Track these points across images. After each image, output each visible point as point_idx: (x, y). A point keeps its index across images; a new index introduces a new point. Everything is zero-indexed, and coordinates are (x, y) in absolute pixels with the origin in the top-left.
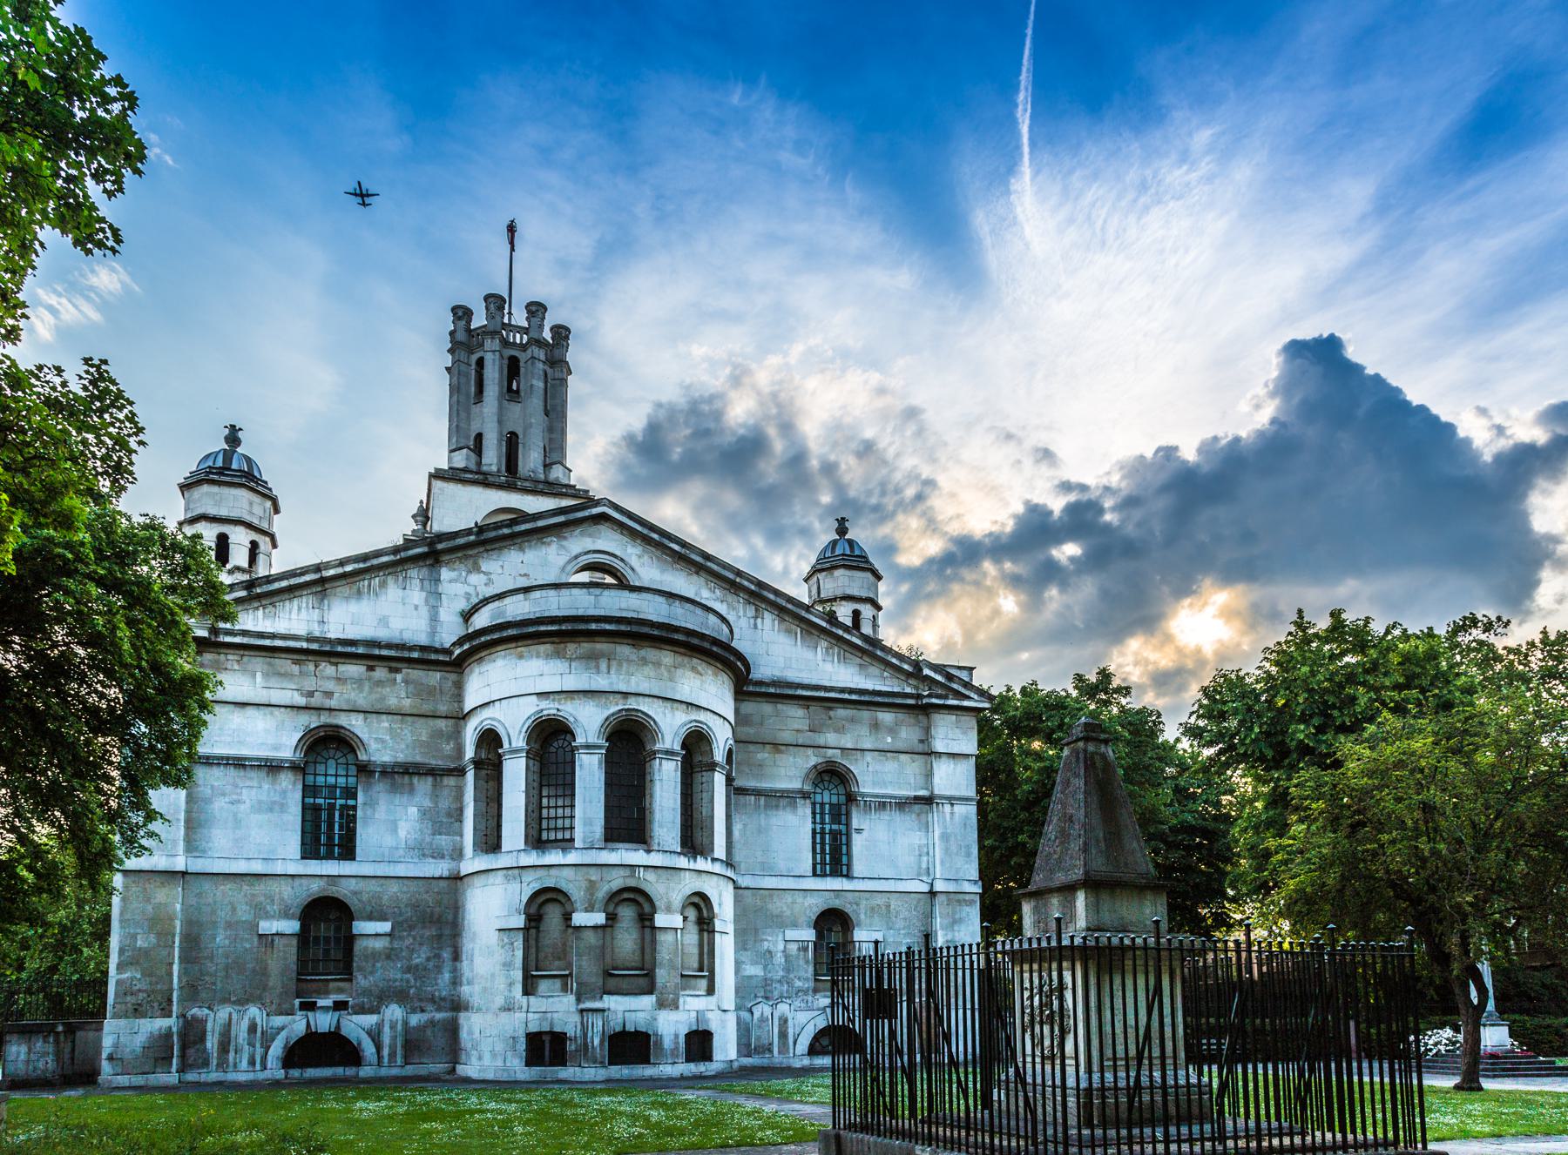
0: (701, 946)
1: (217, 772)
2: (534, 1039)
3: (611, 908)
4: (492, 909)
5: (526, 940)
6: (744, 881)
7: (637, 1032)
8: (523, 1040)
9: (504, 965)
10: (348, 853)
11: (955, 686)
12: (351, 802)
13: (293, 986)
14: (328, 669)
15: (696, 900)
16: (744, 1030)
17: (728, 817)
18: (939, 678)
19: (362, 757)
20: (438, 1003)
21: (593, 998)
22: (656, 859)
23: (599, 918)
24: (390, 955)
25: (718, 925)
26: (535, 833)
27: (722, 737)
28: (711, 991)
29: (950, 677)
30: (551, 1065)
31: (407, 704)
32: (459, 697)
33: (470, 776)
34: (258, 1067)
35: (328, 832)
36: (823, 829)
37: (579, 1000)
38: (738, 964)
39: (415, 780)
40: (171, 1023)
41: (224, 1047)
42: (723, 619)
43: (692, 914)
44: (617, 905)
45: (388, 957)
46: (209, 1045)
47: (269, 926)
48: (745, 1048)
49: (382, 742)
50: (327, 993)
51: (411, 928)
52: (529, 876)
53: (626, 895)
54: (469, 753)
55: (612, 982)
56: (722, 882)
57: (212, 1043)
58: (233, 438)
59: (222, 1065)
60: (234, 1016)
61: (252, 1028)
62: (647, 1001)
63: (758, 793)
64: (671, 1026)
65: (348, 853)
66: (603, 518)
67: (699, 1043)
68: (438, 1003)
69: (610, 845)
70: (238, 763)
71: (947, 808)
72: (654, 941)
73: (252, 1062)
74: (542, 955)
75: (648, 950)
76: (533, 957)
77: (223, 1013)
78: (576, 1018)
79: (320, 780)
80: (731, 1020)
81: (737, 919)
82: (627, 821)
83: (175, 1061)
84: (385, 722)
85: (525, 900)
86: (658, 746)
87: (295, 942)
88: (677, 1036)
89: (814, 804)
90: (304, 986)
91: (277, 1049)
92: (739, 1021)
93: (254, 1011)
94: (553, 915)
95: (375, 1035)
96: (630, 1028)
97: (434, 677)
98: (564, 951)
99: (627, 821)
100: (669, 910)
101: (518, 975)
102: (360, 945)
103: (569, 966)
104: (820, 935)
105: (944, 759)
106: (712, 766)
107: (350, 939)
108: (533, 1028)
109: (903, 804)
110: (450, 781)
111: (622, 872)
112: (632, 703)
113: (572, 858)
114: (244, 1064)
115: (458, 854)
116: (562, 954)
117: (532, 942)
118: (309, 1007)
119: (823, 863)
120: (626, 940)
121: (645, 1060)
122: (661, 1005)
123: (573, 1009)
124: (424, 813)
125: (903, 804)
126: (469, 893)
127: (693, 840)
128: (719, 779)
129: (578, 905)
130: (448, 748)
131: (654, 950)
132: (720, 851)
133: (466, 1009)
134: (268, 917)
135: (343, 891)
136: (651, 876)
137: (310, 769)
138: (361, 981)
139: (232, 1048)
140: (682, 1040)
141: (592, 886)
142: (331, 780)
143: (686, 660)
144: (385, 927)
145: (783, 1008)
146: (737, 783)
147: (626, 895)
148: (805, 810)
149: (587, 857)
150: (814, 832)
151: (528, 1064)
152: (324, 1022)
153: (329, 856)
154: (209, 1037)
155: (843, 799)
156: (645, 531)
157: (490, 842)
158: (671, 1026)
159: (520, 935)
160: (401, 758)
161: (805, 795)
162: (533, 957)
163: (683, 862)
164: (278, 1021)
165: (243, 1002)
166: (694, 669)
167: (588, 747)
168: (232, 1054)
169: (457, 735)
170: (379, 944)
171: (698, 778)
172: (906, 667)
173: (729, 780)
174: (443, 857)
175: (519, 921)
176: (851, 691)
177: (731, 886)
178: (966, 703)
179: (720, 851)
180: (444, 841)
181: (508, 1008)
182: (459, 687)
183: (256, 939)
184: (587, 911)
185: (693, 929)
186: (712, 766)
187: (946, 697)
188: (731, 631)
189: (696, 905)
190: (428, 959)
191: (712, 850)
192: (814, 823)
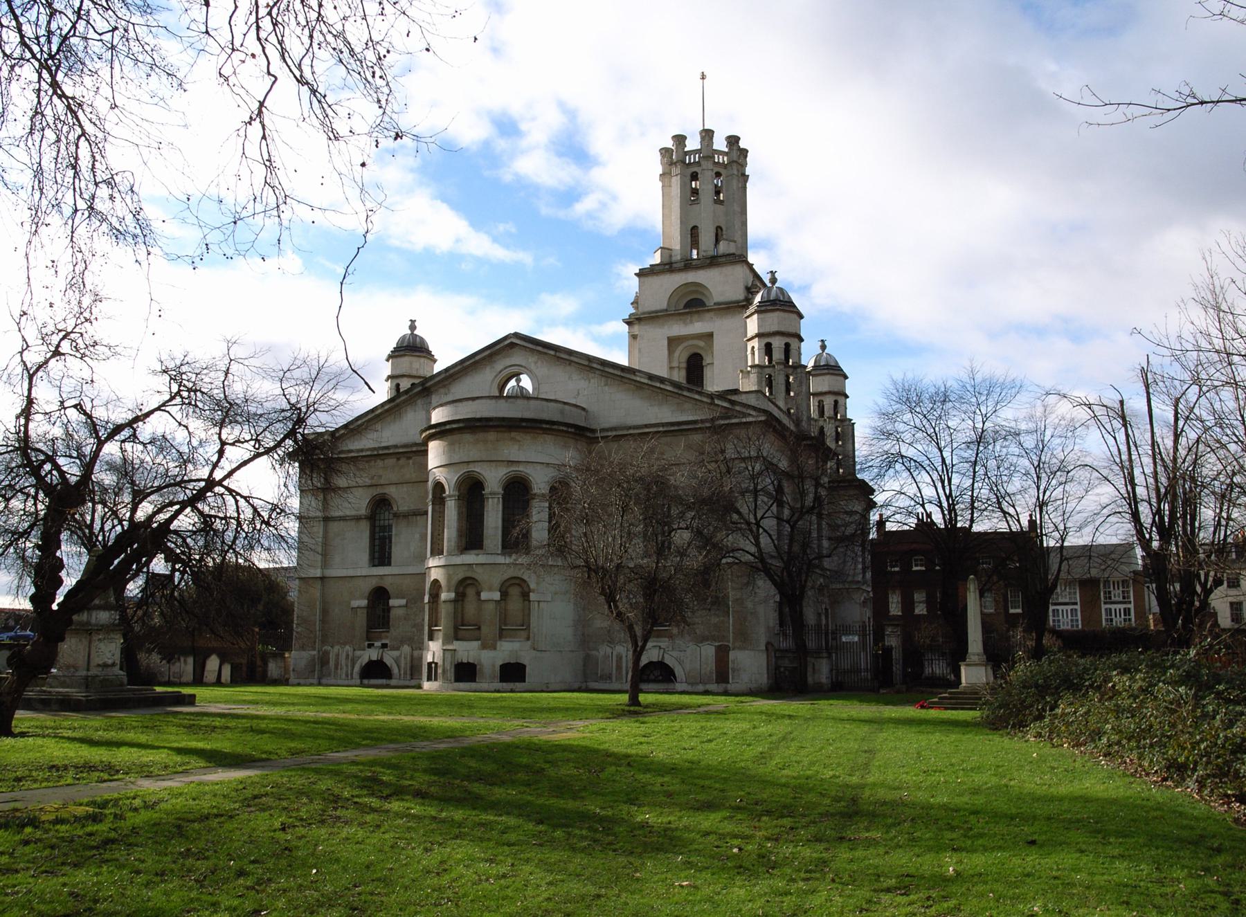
1: (336, 523)
7: (468, 663)
14: (380, 463)
41: (336, 668)
44: (465, 587)
47: (355, 603)
57: (332, 663)
58: (413, 327)
62: (476, 644)
66: (512, 345)
70: (343, 519)
84: (405, 488)
86: (487, 491)
91: (357, 669)
94: (471, 592)
95: (397, 661)
100: (490, 589)
102: (393, 613)
107: (388, 609)
112: (472, 468)
118: (370, 646)
120: (515, 605)
122: (484, 647)
135: (386, 583)
136: (479, 570)
138: (394, 632)
140: (498, 669)
144: (403, 602)
163: (501, 560)
164: (358, 653)
165: (345, 644)
166: (513, 439)
170: (401, 612)
172: (705, 400)
176: (672, 424)
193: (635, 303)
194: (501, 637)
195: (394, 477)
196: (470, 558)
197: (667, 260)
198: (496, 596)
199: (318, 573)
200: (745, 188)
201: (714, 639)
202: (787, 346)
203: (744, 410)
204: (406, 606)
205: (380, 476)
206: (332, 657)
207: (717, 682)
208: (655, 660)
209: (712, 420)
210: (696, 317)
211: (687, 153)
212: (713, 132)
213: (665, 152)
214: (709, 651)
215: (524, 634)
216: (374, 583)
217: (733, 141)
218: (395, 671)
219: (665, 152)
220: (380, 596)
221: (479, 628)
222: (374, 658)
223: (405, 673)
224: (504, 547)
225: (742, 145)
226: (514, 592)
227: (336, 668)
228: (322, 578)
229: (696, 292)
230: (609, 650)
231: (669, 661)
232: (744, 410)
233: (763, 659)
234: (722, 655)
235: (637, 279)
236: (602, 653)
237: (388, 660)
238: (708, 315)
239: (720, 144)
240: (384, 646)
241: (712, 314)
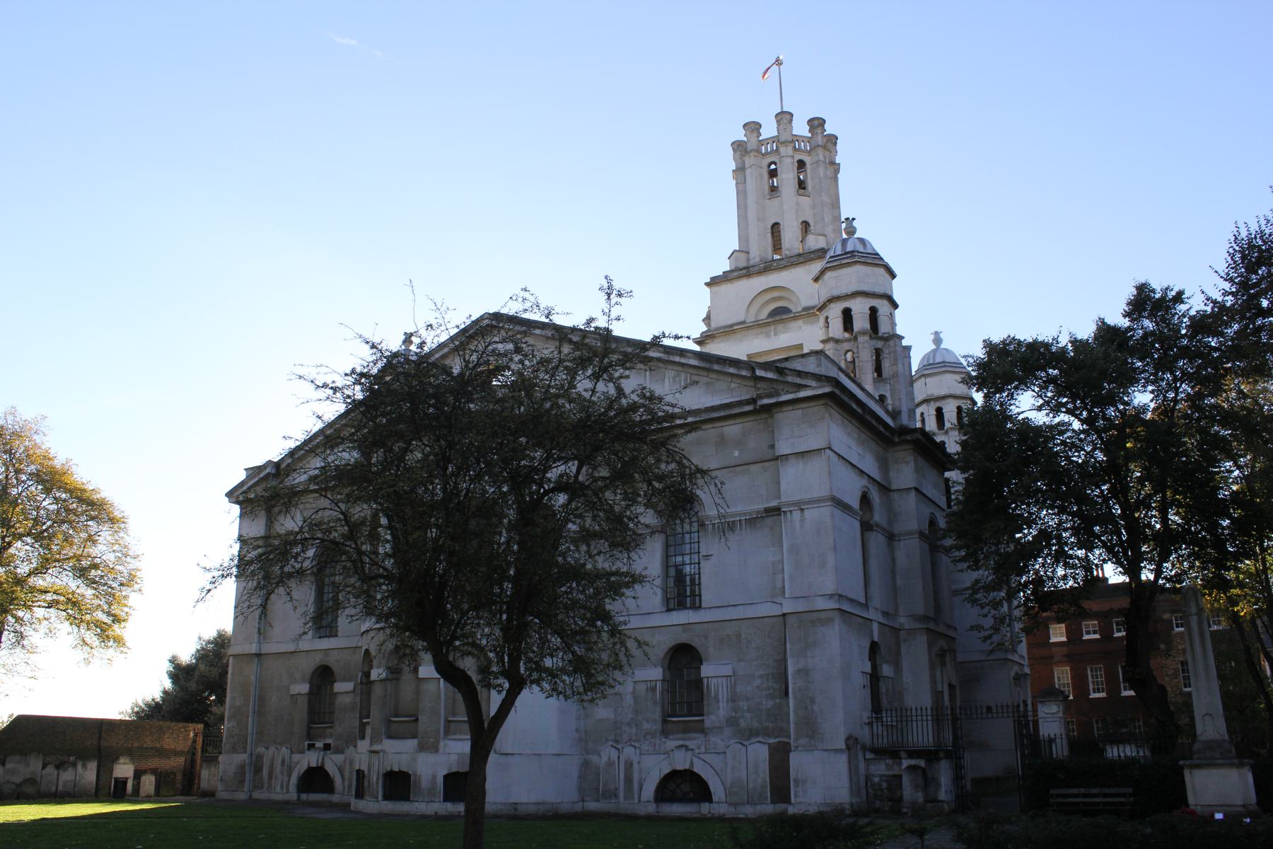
11: (790, 379)
18: (770, 375)
29: (781, 371)
37: (371, 744)
40: (242, 757)
41: (270, 778)
61: (283, 761)
62: (412, 744)
71: (797, 515)
73: (282, 787)
83: (247, 784)
88: (434, 777)
105: (792, 460)
109: (753, 521)
114: (278, 789)
118: (311, 746)
121: (406, 798)
122: (422, 748)
125: (753, 521)
135: (332, 661)
140: (440, 780)
164: (296, 757)
170: (347, 700)
172: (744, 373)
178: (803, 394)
187: (778, 395)
193: (707, 320)
194: (447, 732)
197: (743, 264)
199: (253, 649)
200: (836, 179)
201: (766, 733)
202: (873, 311)
203: (798, 381)
204: (354, 691)
206: (266, 761)
207: (773, 802)
209: (753, 401)
210: (780, 327)
211: (761, 143)
212: (792, 115)
213: (738, 147)
214: (760, 753)
216: (317, 660)
217: (817, 124)
219: (738, 147)
220: (324, 675)
221: (417, 720)
222: (314, 764)
223: (350, 787)
225: (829, 129)
227: (270, 778)
228: (259, 655)
229: (780, 298)
230: (614, 754)
231: (699, 769)
232: (798, 381)
233: (841, 763)
234: (780, 756)
235: (707, 290)
236: (605, 759)
237: (331, 769)
238: (794, 325)
239: (800, 128)
240: (327, 747)
241: (800, 322)
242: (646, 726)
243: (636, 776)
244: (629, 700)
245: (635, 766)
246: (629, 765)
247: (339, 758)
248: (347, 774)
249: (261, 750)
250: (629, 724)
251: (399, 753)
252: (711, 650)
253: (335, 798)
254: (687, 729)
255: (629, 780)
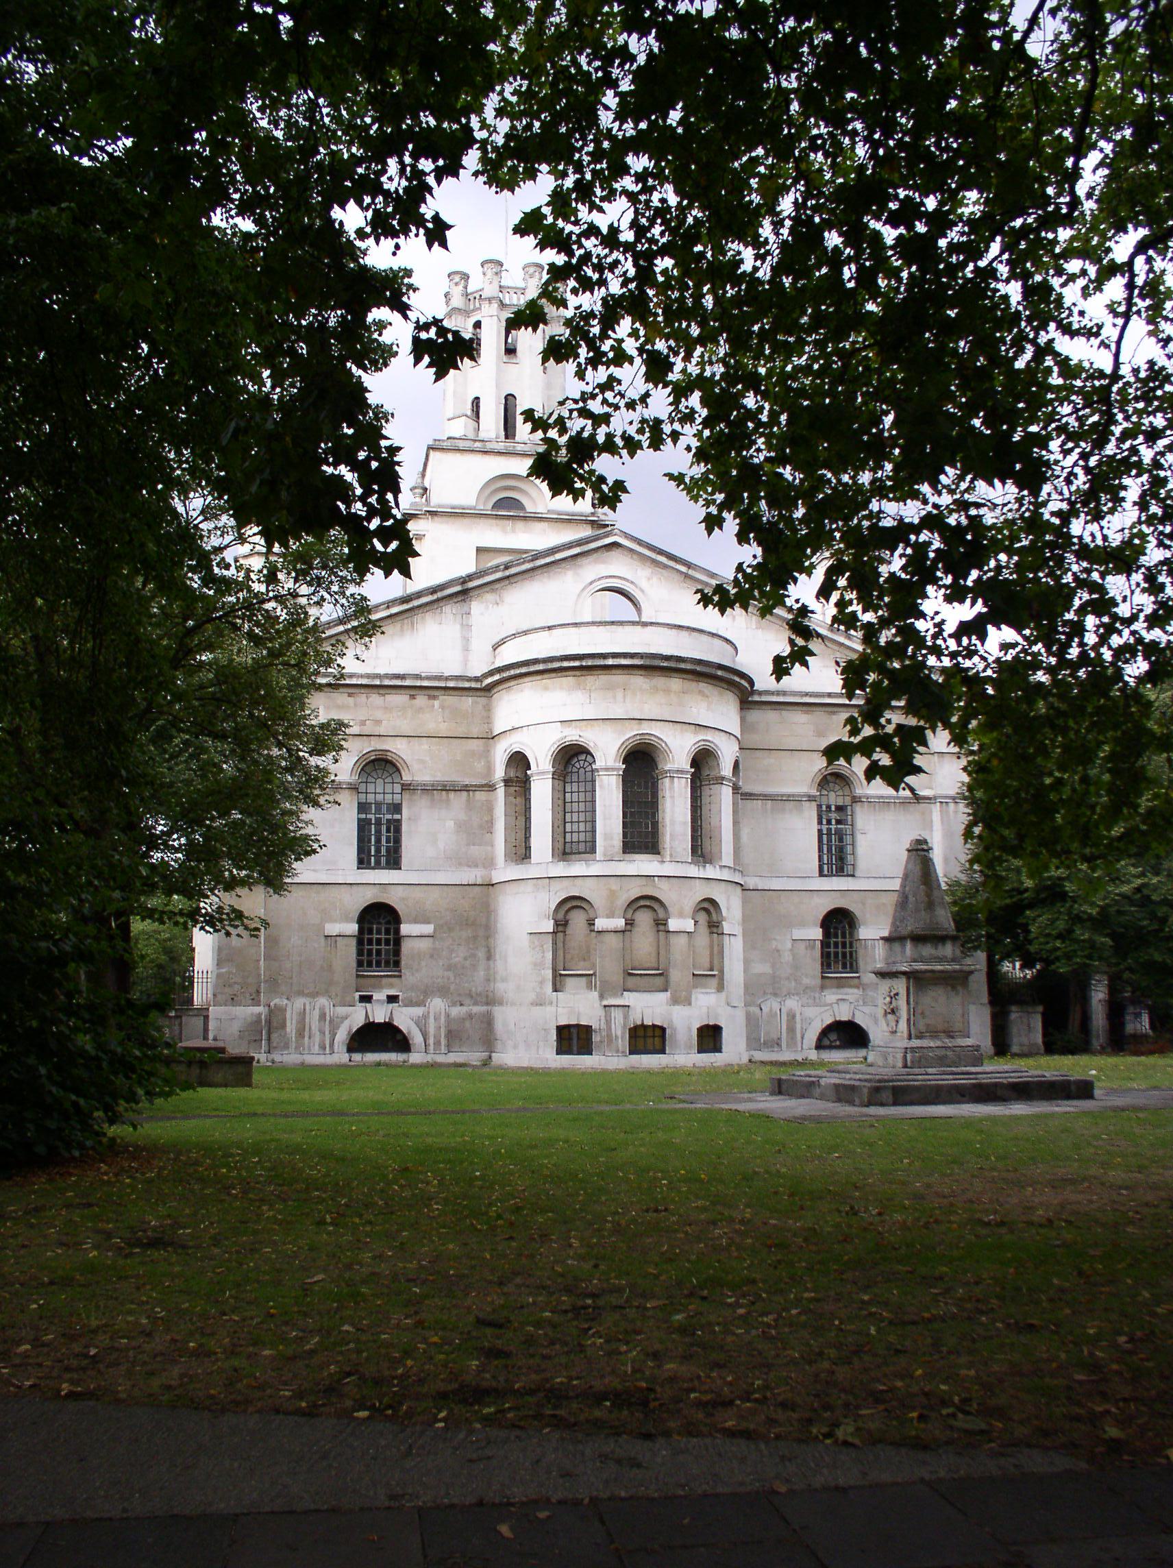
0: (711, 947)
2: (561, 1030)
3: (629, 916)
4: (524, 915)
5: (555, 943)
6: (751, 882)
7: (654, 1026)
8: (555, 1032)
9: (535, 964)
10: (394, 861)
12: (397, 817)
13: (353, 980)
15: (706, 905)
16: (752, 1023)
17: (736, 823)
19: (406, 777)
20: (475, 998)
21: (615, 995)
22: (669, 869)
23: (620, 923)
24: (433, 955)
25: (727, 927)
26: (561, 846)
27: (728, 753)
28: (721, 988)
30: (579, 1053)
31: (444, 728)
32: (488, 719)
33: (501, 791)
34: (328, 1051)
35: (380, 843)
36: (829, 830)
37: (602, 997)
38: (747, 962)
39: (452, 795)
41: (300, 1033)
42: (727, 641)
43: (702, 917)
45: (432, 956)
46: (288, 1030)
47: (333, 928)
48: (754, 1041)
49: (420, 763)
50: (379, 987)
51: (450, 929)
52: (556, 885)
53: (642, 903)
54: (499, 772)
55: (631, 982)
56: (730, 887)
57: (291, 1027)
59: (299, 1048)
60: (307, 1007)
61: (323, 1016)
62: (663, 997)
63: (766, 797)
64: (683, 1021)
65: (394, 861)
66: (615, 545)
67: (710, 1037)
68: (475, 998)
69: (628, 856)
72: (668, 944)
74: (568, 957)
75: (662, 952)
76: (560, 957)
77: (299, 1002)
78: (602, 1012)
79: (371, 798)
80: (740, 1015)
81: (746, 919)
82: (641, 834)
84: (425, 745)
85: (553, 907)
87: (354, 942)
89: (819, 806)
90: (361, 980)
91: (342, 1036)
92: (749, 1017)
93: (323, 1001)
94: (578, 920)
96: (648, 1022)
97: (468, 702)
98: (588, 952)
99: (641, 834)
100: (681, 915)
101: (549, 974)
102: (406, 947)
103: (593, 966)
104: (827, 934)
106: (720, 780)
107: (398, 940)
108: (563, 1022)
110: (480, 796)
111: (639, 881)
112: (646, 729)
113: (595, 869)
114: (316, 1049)
115: (490, 863)
116: (586, 957)
117: (560, 945)
118: (366, 999)
119: (830, 864)
122: (675, 1001)
123: (597, 1004)
124: (460, 826)
126: (501, 898)
127: (701, 850)
128: (726, 793)
129: (600, 912)
130: (479, 766)
131: (668, 951)
132: (727, 858)
133: (501, 1004)
134: (332, 920)
136: (664, 885)
137: (362, 788)
139: (307, 1034)
140: (695, 1033)
141: (612, 894)
142: (380, 797)
143: (694, 684)
144: (428, 929)
145: (792, 1003)
146: (747, 788)
147: (642, 903)
148: (811, 812)
149: (609, 870)
150: (820, 831)
151: (560, 1051)
152: (379, 1014)
153: (378, 866)
154: (288, 1024)
155: (848, 800)
156: (653, 555)
157: (521, 852)
158: (683, 1021)
159: (550, 937)
160: (439, 777)
161: (811, 799)
162: (560, 957)
163: (693, 871)
164: (342, 1010)
165: (314, 995)
166: (701, 692)
167: (607, 769)
168: (306, 1039)
169: (487, 754)
170: (424, 945)
171: (706, 791)
173: (736, 789)
174: (476, 866)
175: (549, 926)
177: (739, 889)
179: (727, 858)
180: (475, 851)
181: (539, 1003)
182: (488, 709)
183: (323, 940)
184: (608, 917)
185: (703, 929)
186: (720, 780)
188: (736, 649)
189: (705, 909)
190: (465, 959)
191: (721, 858)
192: (820, 822)
195: (405, 726)
196: (643, 864)
198: (620, 923)
205: (378, 722)
208: (845, 1018)
211: (501, 288)
215: (714, 982)
216: (368, 897)
218: (417, 1039)
223: (437, 1043)
224: (624, 852)
226: (644, 919)
240: (392, 999)
242: (806, 981)
243: (798, 1026)
244: (787, 957)
245: (798, 1018)
246: (792, 1016)
247: (418, 1011)
248: (431, 1030)
249: (276, 1001)
250: (788, 978)
251: (648, 1006)
252: (868, 916)
253: (415, 1058)
254: (841, 984)
255: (791, 1029)
